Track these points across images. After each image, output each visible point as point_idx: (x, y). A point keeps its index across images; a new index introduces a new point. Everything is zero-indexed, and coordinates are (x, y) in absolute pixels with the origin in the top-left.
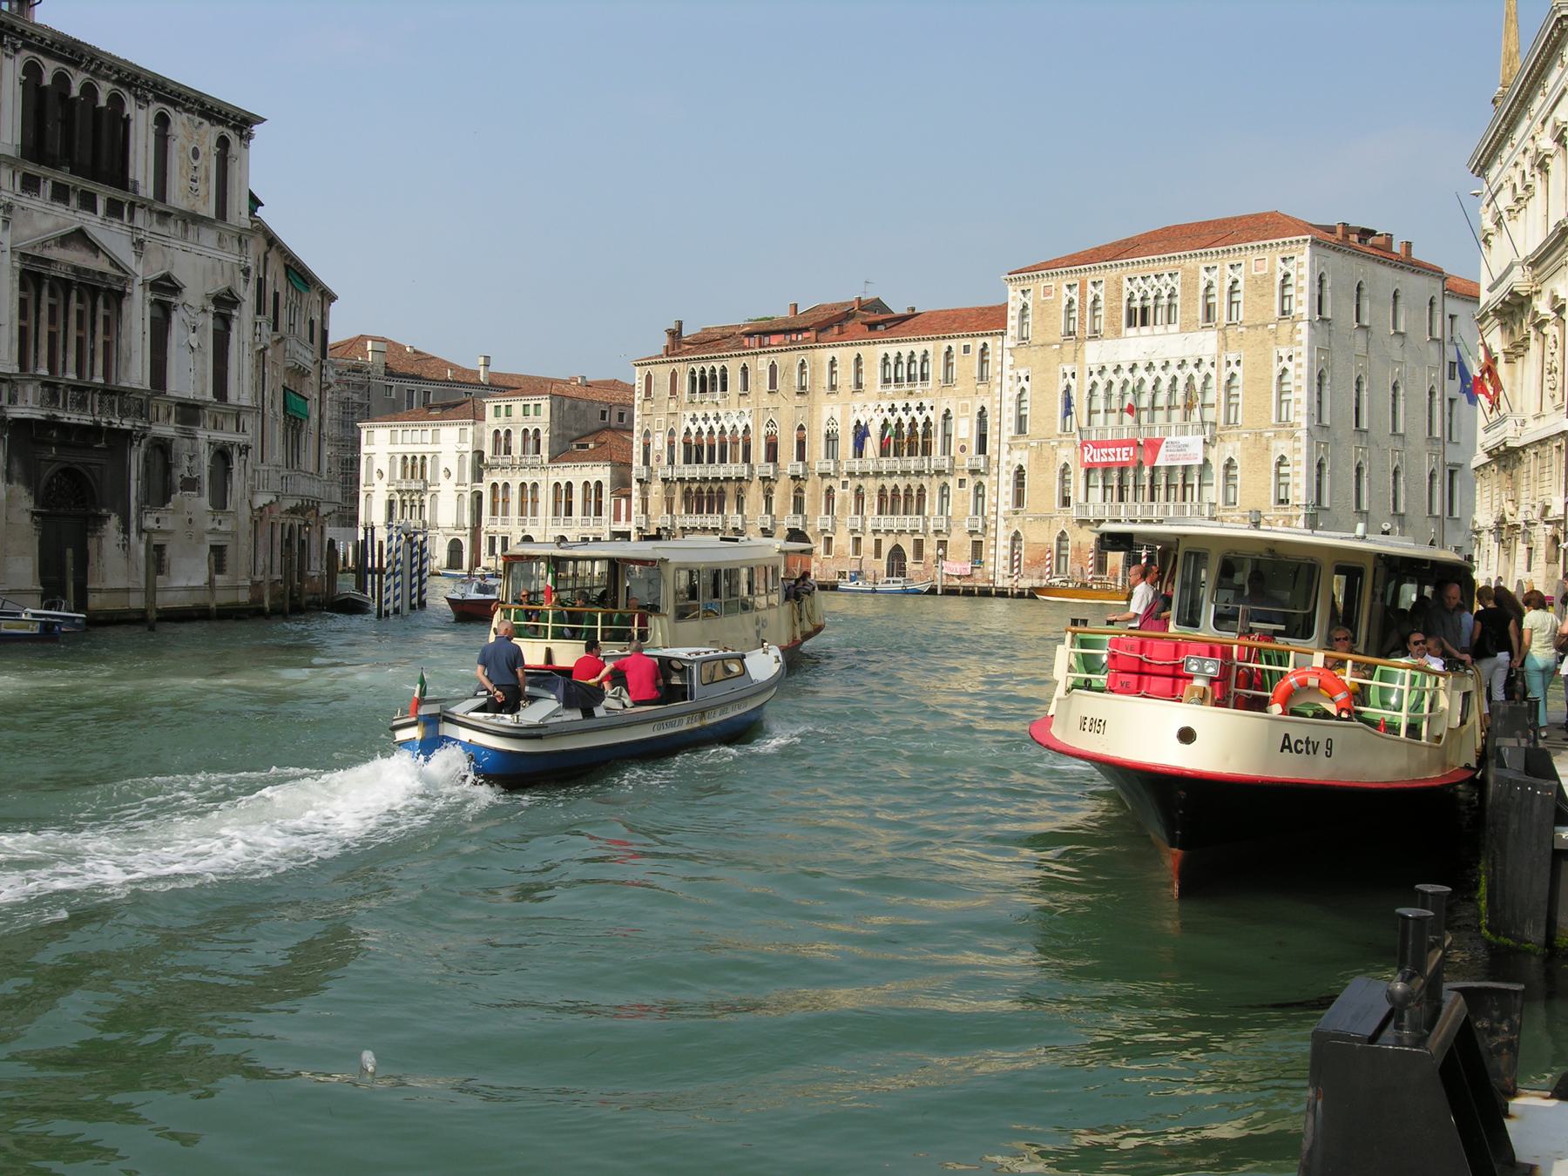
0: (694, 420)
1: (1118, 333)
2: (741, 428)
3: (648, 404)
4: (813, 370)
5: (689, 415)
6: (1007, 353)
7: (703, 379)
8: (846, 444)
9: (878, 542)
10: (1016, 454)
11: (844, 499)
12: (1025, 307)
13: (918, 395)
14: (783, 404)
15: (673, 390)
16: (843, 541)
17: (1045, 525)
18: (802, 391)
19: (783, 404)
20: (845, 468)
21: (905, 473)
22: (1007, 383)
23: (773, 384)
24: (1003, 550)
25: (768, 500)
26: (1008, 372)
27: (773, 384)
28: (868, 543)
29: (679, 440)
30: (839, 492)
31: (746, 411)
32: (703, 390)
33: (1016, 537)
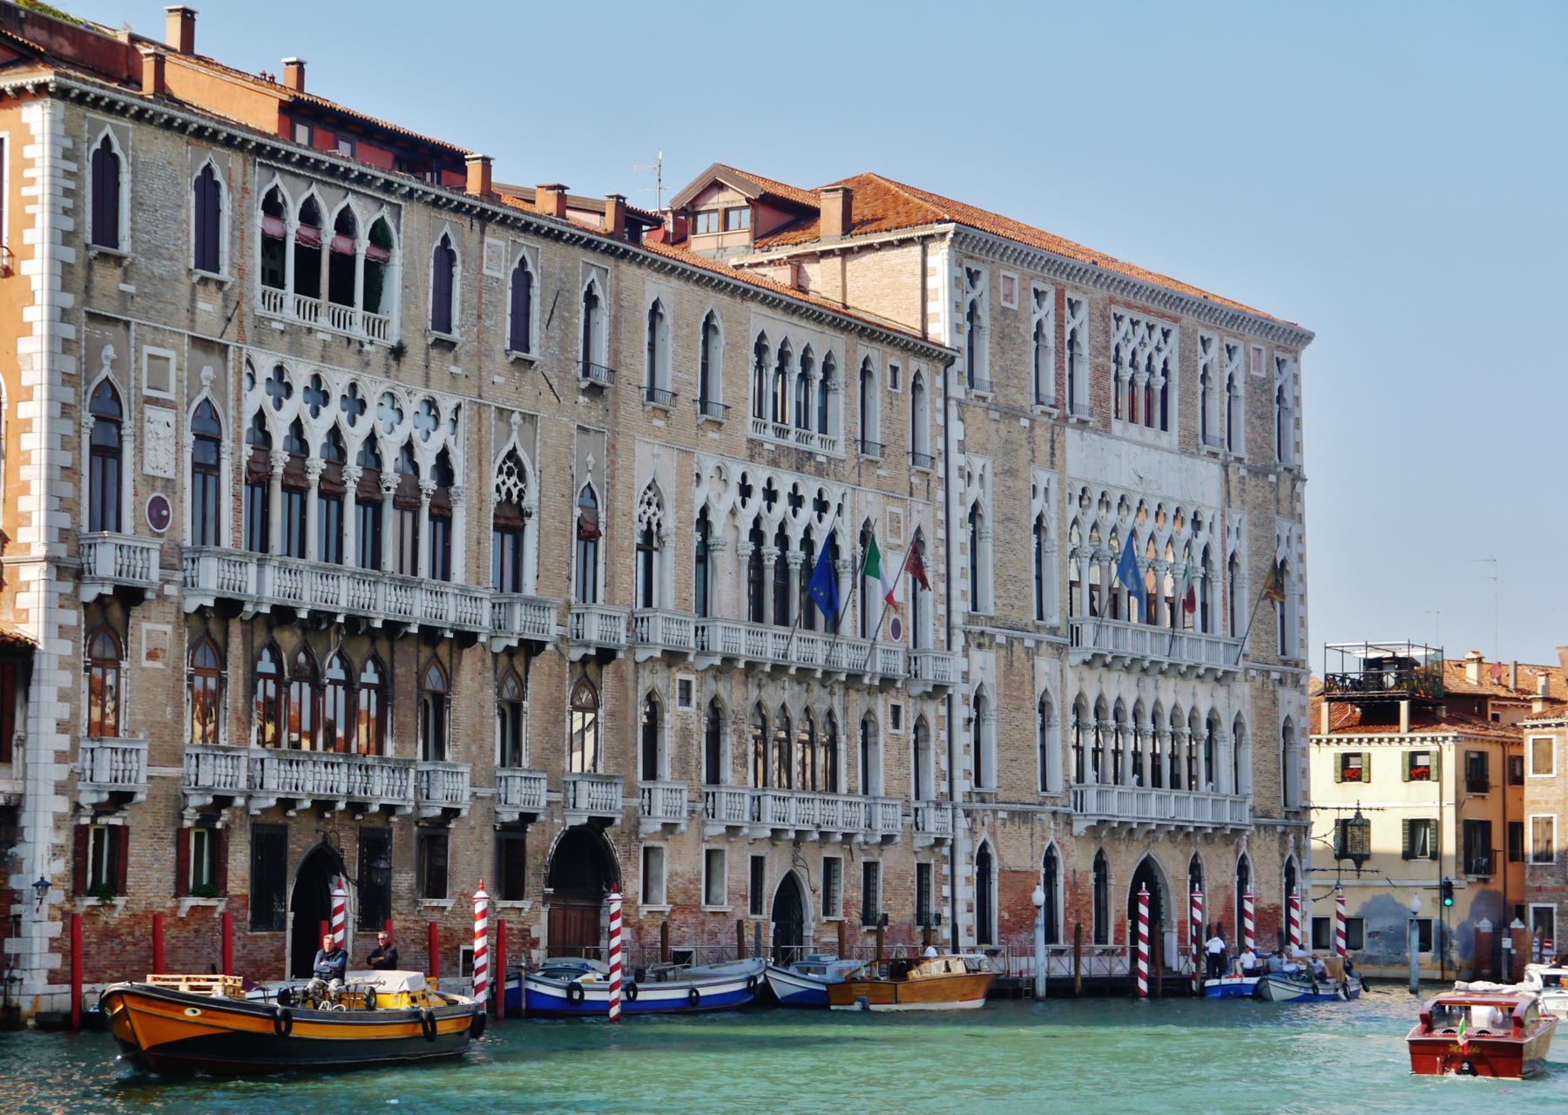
0: (281, 385)
1: (1106, 425)
2: (426, 459)
3: (107, 279)
4: (615, 322)
5: (265, 365)
6: (953, 411)
7: (308, 257)
8: (673, 569)
9: (757, 864)
10: (977, 656)
11: (685, 735)
12: (973, 305)
13: (820, 471)
14: (546, 409)
15: (208, 255)
16: (681, 863)
17: (1025, 831)
18: (595, 391)
19: (546, 409)
20: (718, 644)
21: (804, 674)
22: (957, 484)
23: (520, 339)
24: (967, 893)
25: (512, 714)
26: (956, 459)
27: (520, 339)
28: (736, 872)
29: (235, 455)
30: (673, 715)
31: (446, 406)
32: (307, 285)
33: (983, 859)
